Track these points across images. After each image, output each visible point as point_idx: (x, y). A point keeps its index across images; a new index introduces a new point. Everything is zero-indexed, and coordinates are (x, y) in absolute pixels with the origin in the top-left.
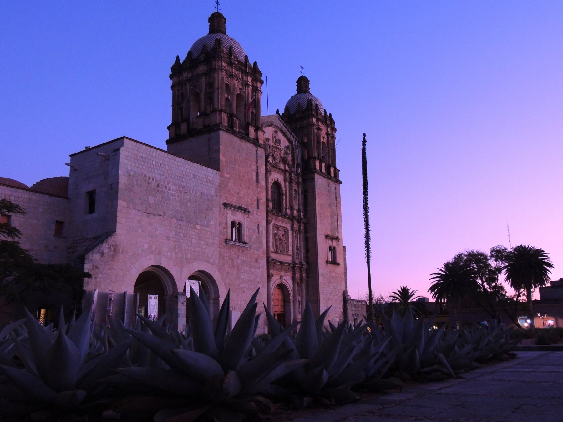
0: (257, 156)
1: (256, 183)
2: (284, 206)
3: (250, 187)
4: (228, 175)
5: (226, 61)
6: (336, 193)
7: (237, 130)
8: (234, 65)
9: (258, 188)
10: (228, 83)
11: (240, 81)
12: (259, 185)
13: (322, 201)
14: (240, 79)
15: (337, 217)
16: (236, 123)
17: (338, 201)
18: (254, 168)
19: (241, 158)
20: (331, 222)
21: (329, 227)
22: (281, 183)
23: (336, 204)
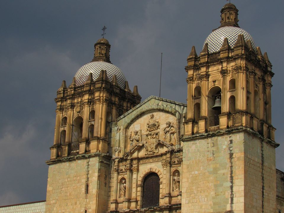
0: (88, 168)
1: (85, 195)
2: (160, 196)
3: (78, 202)
4: (54, 201)
5: (59, 100)
6: (231, 149)
7: (66, 155)
8: (67, 97)
9: (86, 199)
10: (65, 116)
11: (78, 105)
12: (89, 195)
13: (196, 172)
14: (78, 103)
15: (232, 182)
16: (66, 149)
17: (236, 159)
18: (84, 181)
19: (69, 179)
20: (214, 195)
21: (211, 203)
22: (156, 172)
23: (229, 165)
